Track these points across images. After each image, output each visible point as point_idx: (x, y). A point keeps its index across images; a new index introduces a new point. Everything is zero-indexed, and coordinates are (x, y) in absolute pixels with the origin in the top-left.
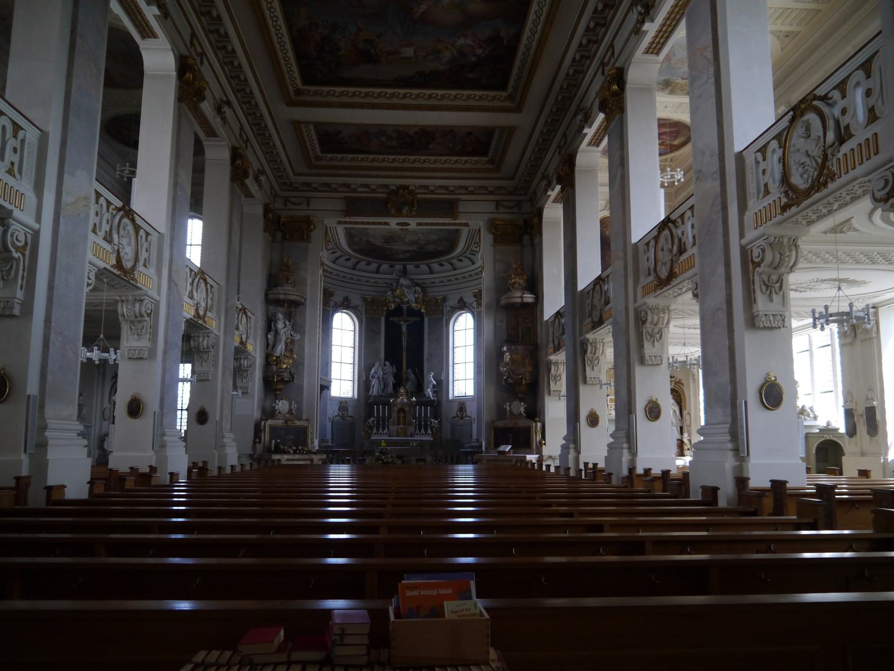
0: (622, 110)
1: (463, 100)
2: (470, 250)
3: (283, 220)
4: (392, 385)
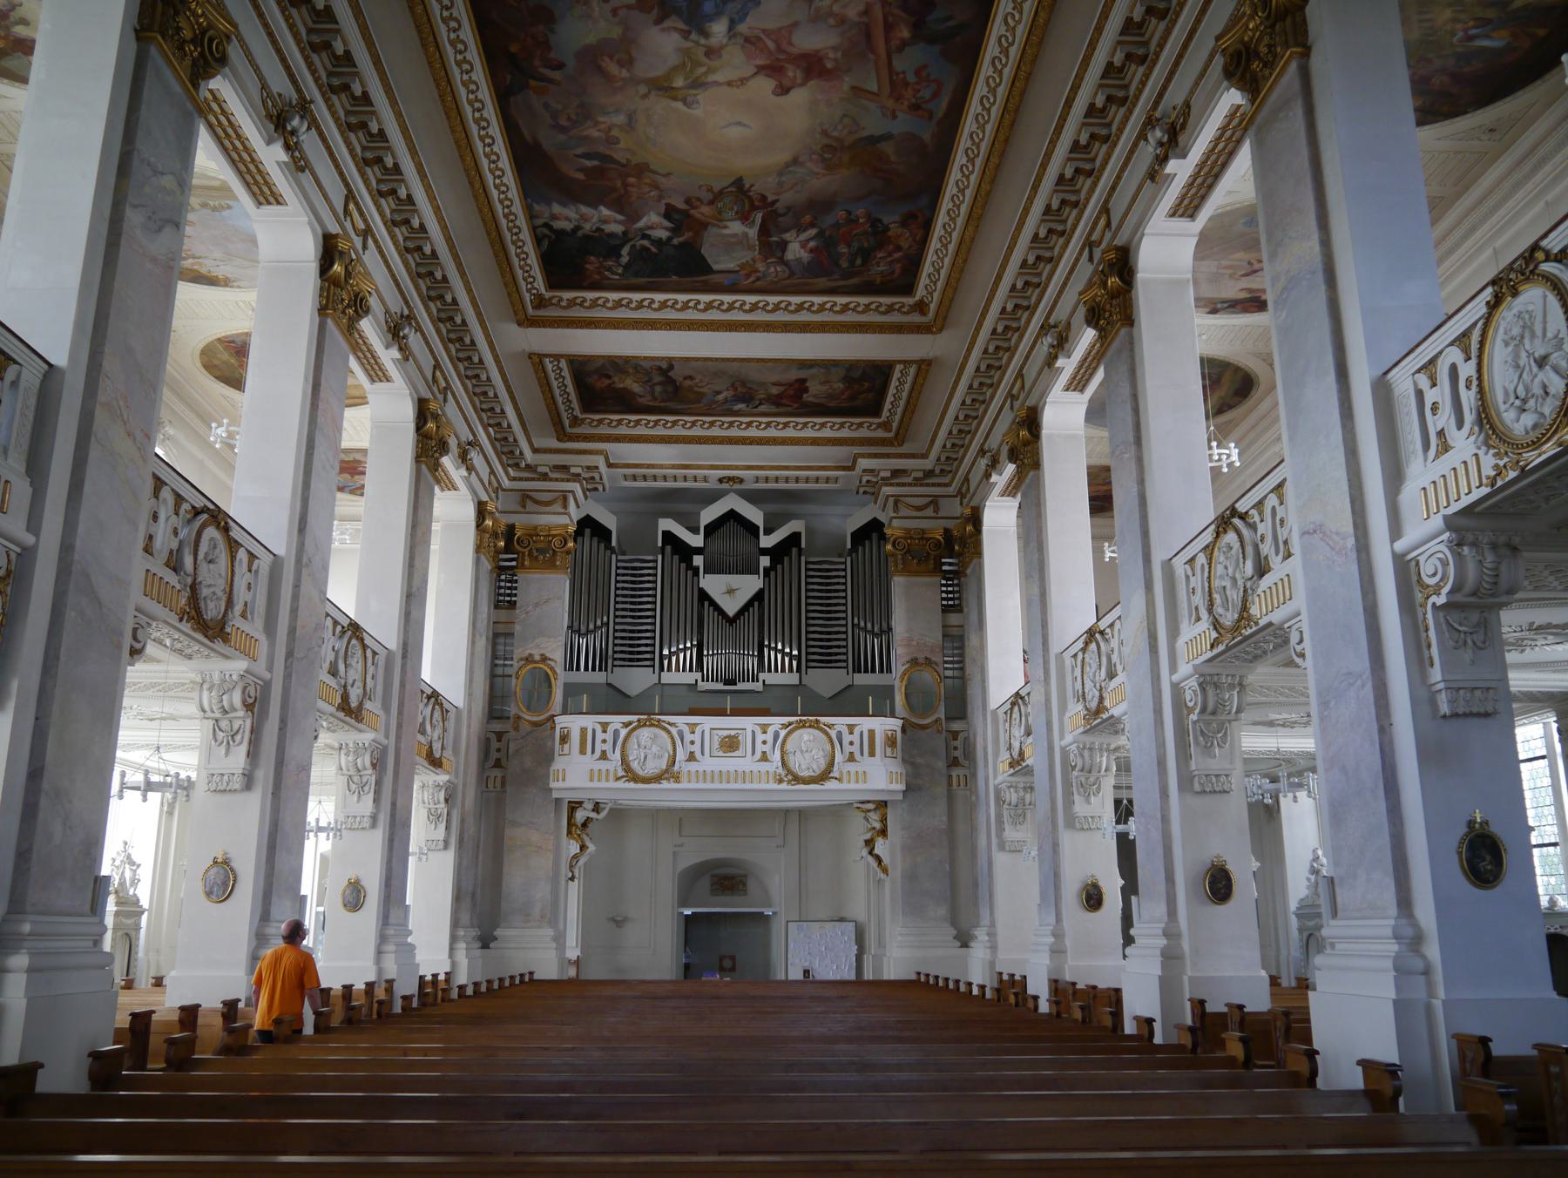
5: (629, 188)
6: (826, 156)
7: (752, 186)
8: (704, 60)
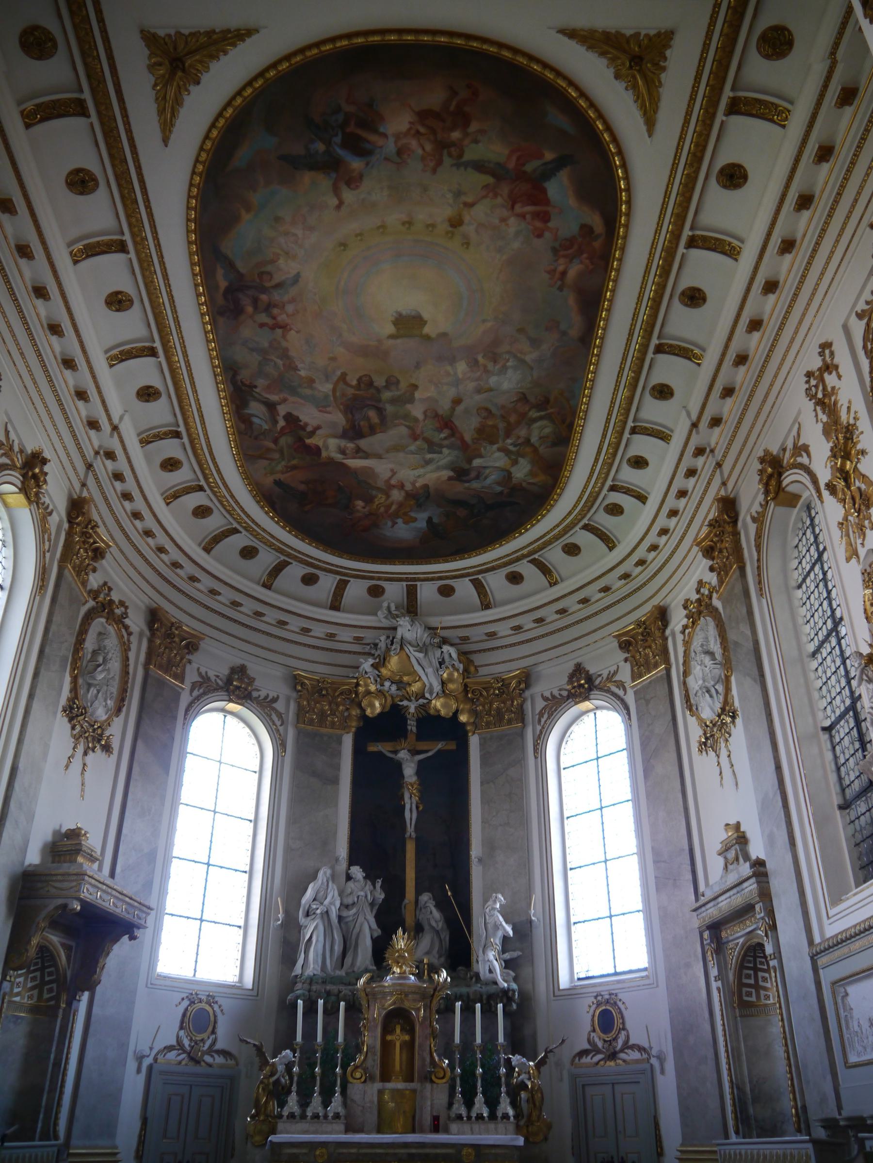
4: (369, 943)
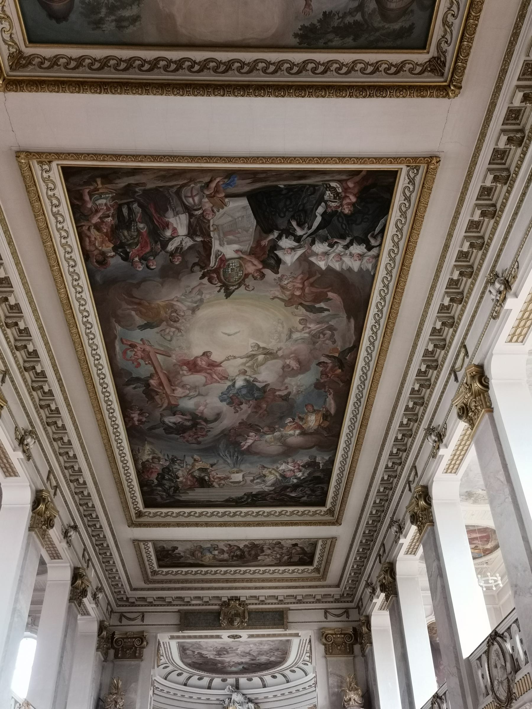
0: (432, 523)
1: (288, 516)
2: (302, 660)
3: (116, 637)
5: (301, 286)
6: (175, 315)
7: (219, 291)
8: (246, 369)
